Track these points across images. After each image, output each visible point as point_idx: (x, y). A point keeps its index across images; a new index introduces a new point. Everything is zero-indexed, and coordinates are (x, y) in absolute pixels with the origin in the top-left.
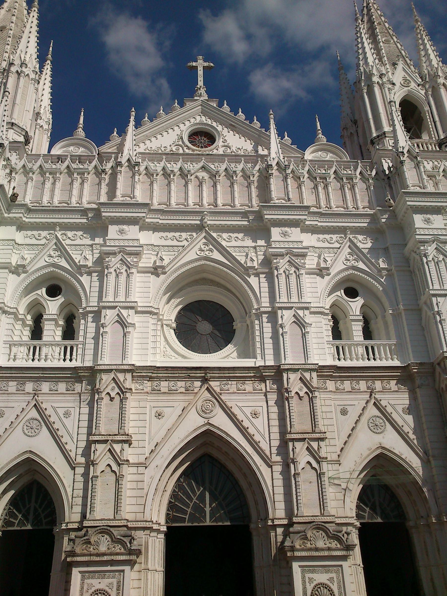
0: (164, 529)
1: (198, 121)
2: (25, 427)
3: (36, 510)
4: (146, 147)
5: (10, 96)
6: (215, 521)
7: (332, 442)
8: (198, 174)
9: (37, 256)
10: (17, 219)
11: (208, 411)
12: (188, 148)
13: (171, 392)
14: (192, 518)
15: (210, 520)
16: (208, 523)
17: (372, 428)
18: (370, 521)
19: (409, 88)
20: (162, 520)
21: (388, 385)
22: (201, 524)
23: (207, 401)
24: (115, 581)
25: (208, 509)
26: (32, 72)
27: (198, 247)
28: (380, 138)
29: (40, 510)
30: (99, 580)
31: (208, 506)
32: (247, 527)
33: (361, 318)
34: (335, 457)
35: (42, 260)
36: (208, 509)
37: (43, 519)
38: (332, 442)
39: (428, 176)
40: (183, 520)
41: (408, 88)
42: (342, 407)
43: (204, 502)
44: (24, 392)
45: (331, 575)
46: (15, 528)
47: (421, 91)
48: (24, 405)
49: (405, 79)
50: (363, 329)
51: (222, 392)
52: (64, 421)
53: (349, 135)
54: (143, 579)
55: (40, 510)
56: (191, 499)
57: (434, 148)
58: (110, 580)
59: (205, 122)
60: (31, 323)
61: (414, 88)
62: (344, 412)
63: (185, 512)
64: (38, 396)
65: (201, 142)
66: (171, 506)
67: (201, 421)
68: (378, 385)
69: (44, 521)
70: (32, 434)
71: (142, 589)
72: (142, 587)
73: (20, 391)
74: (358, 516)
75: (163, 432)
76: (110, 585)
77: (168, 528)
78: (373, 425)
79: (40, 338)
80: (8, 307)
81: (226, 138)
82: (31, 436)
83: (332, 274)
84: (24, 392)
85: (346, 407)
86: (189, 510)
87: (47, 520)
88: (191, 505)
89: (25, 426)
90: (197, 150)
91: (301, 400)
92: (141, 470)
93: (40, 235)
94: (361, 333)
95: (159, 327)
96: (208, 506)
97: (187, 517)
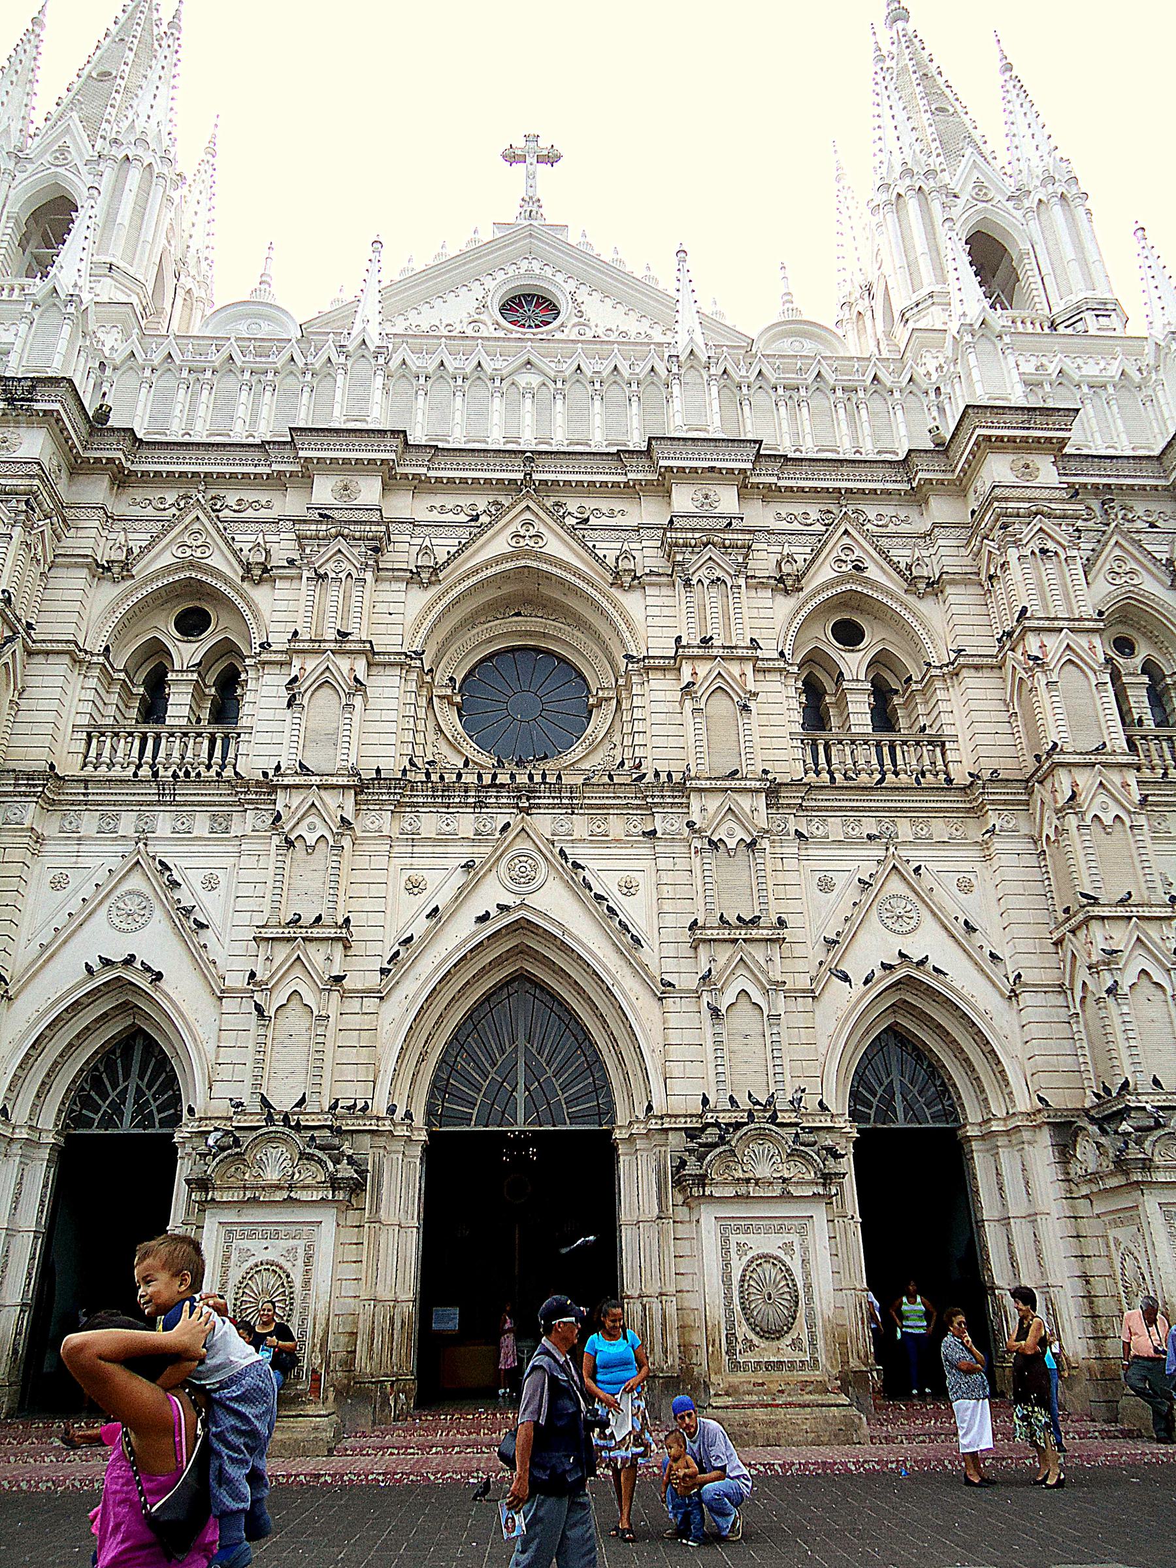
1: (522, 271)
2: (114, 911)
3: (139, 1092)
4: (407, 323)
5: (99, 200)
7: (799, 950)
8: (516, 378)
9: (154, 540)
10: (110, 460)
11: (523, 880)
13: (442, 840)
15: (525, 1120)
17: (889, 922)
19: (988, 205)
21: (926, 829)
23: (521, 859)
24: (300, 1244)
25: (521, 1095)
26: (159, 161)
27: (512, 529)
28: (920, 307)
29: (149, 1095)
30: (265, 1243)
32: (609, 1133)
33: (869, 686)
34: (804, 982)
35: (168, 553)
36: (521, 1095)
37: (155, 1113)
38: (799, 950)
39: (1026, 384)
41: (984, 204)
44: (114, 835)
45: (788, 1238)
46: (95, 1131)
47: (1015, 212)
49: (979, 186)
50: (873, 710)
51: (556, 838)
52: (203, 899)
53: (854, 317)
54: (366, 1243)
55: (149, 1095)
57: (1039, 331)
58: (292, 1243)
59: (537, 271)
60: (142, 690)
61: (999, 205)
64: (146, 844)
65: (529, 317)
66: (438, 1087)
68: (905, 830)
69: (157, 1117)
70: (129, 927)
71: (364, 1263)
72: (364, 1259)
73: (108, 831)
74: (855, 1115)
77: (431, 1134)
78: (889, 914)
79: (161, 720)
80: (86, 652)
81: (583, 308)
82: (127, 931)
83: (806, 591)
84: (114, 835)
85: (829, 874)
87: (162, 1115)
89: (114, 909)
90: (517, 332)
91: (560, 157)
92: (371, 1004)
93: (162, 500)
94: (868, 719)
95: (423, 702)
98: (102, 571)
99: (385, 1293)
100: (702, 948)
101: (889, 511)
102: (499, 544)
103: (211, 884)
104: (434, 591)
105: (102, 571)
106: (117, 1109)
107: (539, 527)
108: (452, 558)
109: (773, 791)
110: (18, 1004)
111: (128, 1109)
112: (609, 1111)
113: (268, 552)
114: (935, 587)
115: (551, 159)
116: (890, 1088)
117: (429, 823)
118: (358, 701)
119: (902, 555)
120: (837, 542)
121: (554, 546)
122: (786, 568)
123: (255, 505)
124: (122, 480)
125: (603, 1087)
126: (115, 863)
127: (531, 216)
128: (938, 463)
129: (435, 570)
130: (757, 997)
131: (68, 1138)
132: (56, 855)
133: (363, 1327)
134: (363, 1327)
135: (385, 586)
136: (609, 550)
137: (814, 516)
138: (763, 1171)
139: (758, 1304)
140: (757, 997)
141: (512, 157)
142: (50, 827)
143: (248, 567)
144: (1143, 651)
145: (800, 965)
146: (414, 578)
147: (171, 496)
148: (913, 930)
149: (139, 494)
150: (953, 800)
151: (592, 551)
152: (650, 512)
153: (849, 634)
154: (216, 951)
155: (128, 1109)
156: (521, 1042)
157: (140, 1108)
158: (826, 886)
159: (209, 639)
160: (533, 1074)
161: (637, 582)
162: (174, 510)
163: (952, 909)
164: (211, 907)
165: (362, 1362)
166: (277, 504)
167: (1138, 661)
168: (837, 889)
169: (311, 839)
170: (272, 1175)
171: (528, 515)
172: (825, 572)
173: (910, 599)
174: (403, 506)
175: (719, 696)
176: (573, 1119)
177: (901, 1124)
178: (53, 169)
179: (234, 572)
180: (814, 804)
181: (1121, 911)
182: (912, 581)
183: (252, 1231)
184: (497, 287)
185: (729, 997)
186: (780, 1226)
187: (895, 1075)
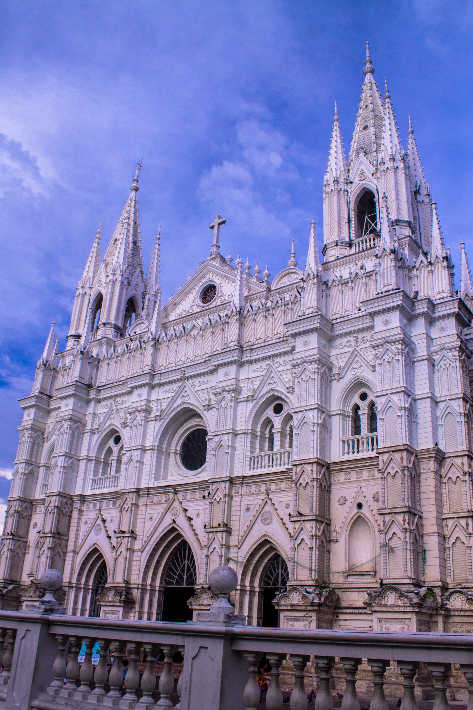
6: (187, 585)
14: (178, 583)
16: (184, 585)
18: (273, 587)
22: (181, 586)
25: (185, 577)
31: (185, 574)
36: (185, 577)
40: (172, 583)
42: (246, 506)
56: (177, 570)
62: (248, 510)
63: (173, 578)
68: (273, 487)
86: (176, 577)
88: (178, 574)
96: (185, 574)
97: (175, 582)
116: (278, 575)
117: (155, 499)
148: (268, 524)
168: (250, 511)
180: (246, 482)
187: (280, 570)
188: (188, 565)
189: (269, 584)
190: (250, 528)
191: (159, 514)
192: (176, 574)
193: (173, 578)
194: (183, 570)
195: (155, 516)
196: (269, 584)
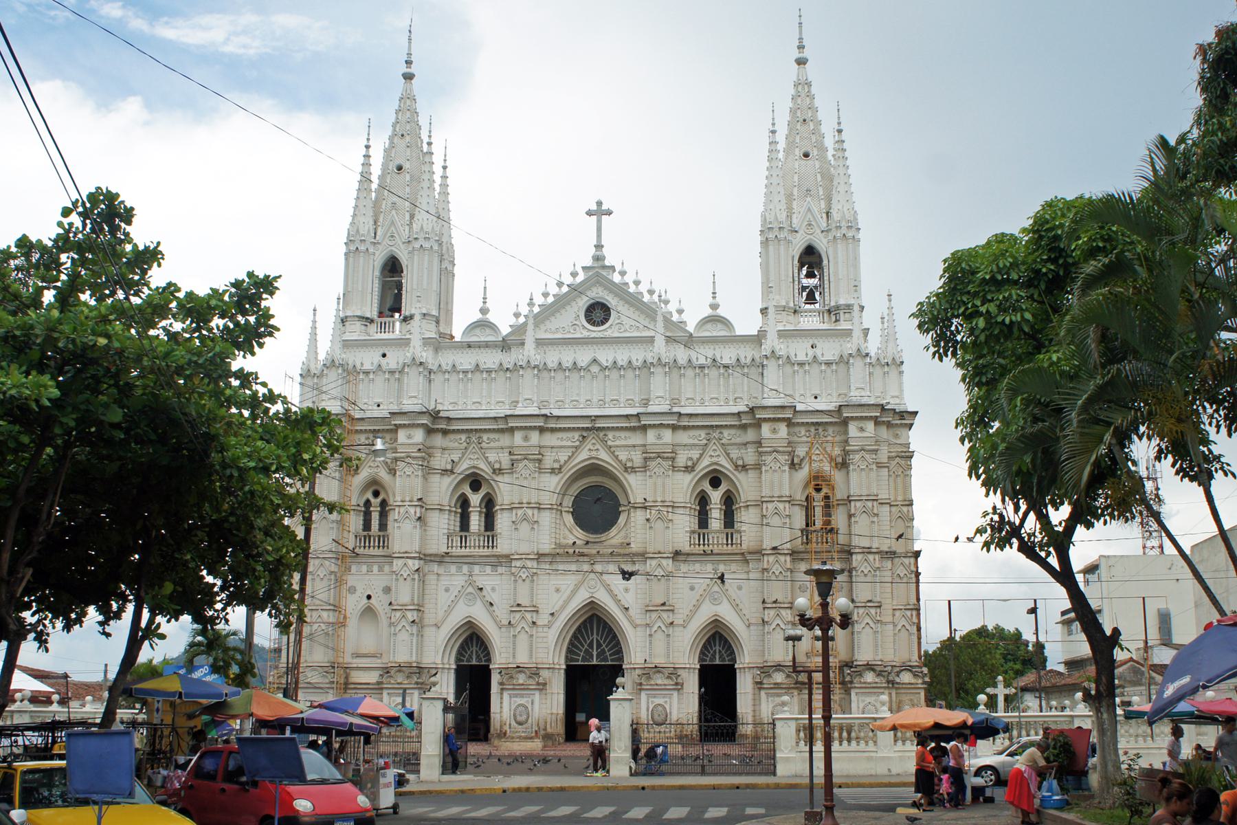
0: (564, 667)
12: (584, 327)
16: (595, 662)
20: (563, 661)
25: (595, 653)
27: (588, 448)
36: (595, 653)
40: (578, 660)
43: (592, 648)
48: (463, 583)
56: (583, 646)
66: (569, 651)
67: (587, 595)
73: (459, 569)
75: (561, 603)
76: (527, 702)
77: (567, 666)
95: (558, 517)
98: (445, 472)
99: (555, 711)
100: (648, 614)
101: (733, 431)
102: (583, 455)
103: (493, 589)
104: (561, 475)
105: (445, 472)
106: (471, 657)
107: (598, 446)
108: (566, 462)
109: (677, 554)
110: (442, 628)
111: (474, 657)
112: (621, 659)
113: (500, 463)
114: (744, 468)
115: (609, 213)
116: (715, 652)
118: (535, 526)
119: (735, 453)
120: (712, 447)
121: (603, 455)
122: (690, 463)
123: (494, 440)
124: (445, 432)
125: (620, 651)
126: (463, 583)
127: (598, 258)
128: (749, 416)
129: (560, 469)
130: (664, 628)
131: (458, 666)
132: (445, 581)
133: (549, 720)
134: (549, 720)
135: (542, 475)
136: (623, 456)
137: (703, 435)
138: (659, 682)
139: (656, 717)
140: (664, 628)
141: (590, 213)
142: (441, 571)
143: (494, 470)
144: (825, 491)
145: (681, 616)
146: (553, 471)
147: (463, 437)
149: (452, 436)
150: (738, 558)
151: (617, 457)
152: (636, 439)
153: (715, 483)
154: (497, 613)
155: (474, 657)
156: (595, 636)
157: (478, 656)
158: (692, 589)
159: (482, 492)
160: (599, 645)
161: (632, 470)
162: (465, 444)
163: (734, 596)
164: (494, 597)
165: (549, 730)
166: (502, 440)
167: (822, 494)
169: (524, 576)
170: (521, 681)
171: (594, 441)
172: (706, 462)
173: (736, 473)
174: (550, 439)
175: (659, 521)
176: (612, 660)
177: (717, 662)
178: (391, 248)
179: (489, 471)
181: (774, 605)
182: (737, 466)
183: (516, 695)
184: (583, 303)
185: (655, 628)
186: (664, 696)
188: (597, 640)
189: (706, 660)
190: (697, 607)
191: (569, 585)
192: (581, 651)
193: (579, 655)
194: (591, 645)
195: (563, 588)
196: (706, 660)
